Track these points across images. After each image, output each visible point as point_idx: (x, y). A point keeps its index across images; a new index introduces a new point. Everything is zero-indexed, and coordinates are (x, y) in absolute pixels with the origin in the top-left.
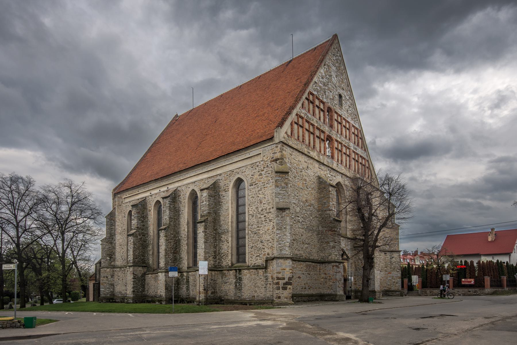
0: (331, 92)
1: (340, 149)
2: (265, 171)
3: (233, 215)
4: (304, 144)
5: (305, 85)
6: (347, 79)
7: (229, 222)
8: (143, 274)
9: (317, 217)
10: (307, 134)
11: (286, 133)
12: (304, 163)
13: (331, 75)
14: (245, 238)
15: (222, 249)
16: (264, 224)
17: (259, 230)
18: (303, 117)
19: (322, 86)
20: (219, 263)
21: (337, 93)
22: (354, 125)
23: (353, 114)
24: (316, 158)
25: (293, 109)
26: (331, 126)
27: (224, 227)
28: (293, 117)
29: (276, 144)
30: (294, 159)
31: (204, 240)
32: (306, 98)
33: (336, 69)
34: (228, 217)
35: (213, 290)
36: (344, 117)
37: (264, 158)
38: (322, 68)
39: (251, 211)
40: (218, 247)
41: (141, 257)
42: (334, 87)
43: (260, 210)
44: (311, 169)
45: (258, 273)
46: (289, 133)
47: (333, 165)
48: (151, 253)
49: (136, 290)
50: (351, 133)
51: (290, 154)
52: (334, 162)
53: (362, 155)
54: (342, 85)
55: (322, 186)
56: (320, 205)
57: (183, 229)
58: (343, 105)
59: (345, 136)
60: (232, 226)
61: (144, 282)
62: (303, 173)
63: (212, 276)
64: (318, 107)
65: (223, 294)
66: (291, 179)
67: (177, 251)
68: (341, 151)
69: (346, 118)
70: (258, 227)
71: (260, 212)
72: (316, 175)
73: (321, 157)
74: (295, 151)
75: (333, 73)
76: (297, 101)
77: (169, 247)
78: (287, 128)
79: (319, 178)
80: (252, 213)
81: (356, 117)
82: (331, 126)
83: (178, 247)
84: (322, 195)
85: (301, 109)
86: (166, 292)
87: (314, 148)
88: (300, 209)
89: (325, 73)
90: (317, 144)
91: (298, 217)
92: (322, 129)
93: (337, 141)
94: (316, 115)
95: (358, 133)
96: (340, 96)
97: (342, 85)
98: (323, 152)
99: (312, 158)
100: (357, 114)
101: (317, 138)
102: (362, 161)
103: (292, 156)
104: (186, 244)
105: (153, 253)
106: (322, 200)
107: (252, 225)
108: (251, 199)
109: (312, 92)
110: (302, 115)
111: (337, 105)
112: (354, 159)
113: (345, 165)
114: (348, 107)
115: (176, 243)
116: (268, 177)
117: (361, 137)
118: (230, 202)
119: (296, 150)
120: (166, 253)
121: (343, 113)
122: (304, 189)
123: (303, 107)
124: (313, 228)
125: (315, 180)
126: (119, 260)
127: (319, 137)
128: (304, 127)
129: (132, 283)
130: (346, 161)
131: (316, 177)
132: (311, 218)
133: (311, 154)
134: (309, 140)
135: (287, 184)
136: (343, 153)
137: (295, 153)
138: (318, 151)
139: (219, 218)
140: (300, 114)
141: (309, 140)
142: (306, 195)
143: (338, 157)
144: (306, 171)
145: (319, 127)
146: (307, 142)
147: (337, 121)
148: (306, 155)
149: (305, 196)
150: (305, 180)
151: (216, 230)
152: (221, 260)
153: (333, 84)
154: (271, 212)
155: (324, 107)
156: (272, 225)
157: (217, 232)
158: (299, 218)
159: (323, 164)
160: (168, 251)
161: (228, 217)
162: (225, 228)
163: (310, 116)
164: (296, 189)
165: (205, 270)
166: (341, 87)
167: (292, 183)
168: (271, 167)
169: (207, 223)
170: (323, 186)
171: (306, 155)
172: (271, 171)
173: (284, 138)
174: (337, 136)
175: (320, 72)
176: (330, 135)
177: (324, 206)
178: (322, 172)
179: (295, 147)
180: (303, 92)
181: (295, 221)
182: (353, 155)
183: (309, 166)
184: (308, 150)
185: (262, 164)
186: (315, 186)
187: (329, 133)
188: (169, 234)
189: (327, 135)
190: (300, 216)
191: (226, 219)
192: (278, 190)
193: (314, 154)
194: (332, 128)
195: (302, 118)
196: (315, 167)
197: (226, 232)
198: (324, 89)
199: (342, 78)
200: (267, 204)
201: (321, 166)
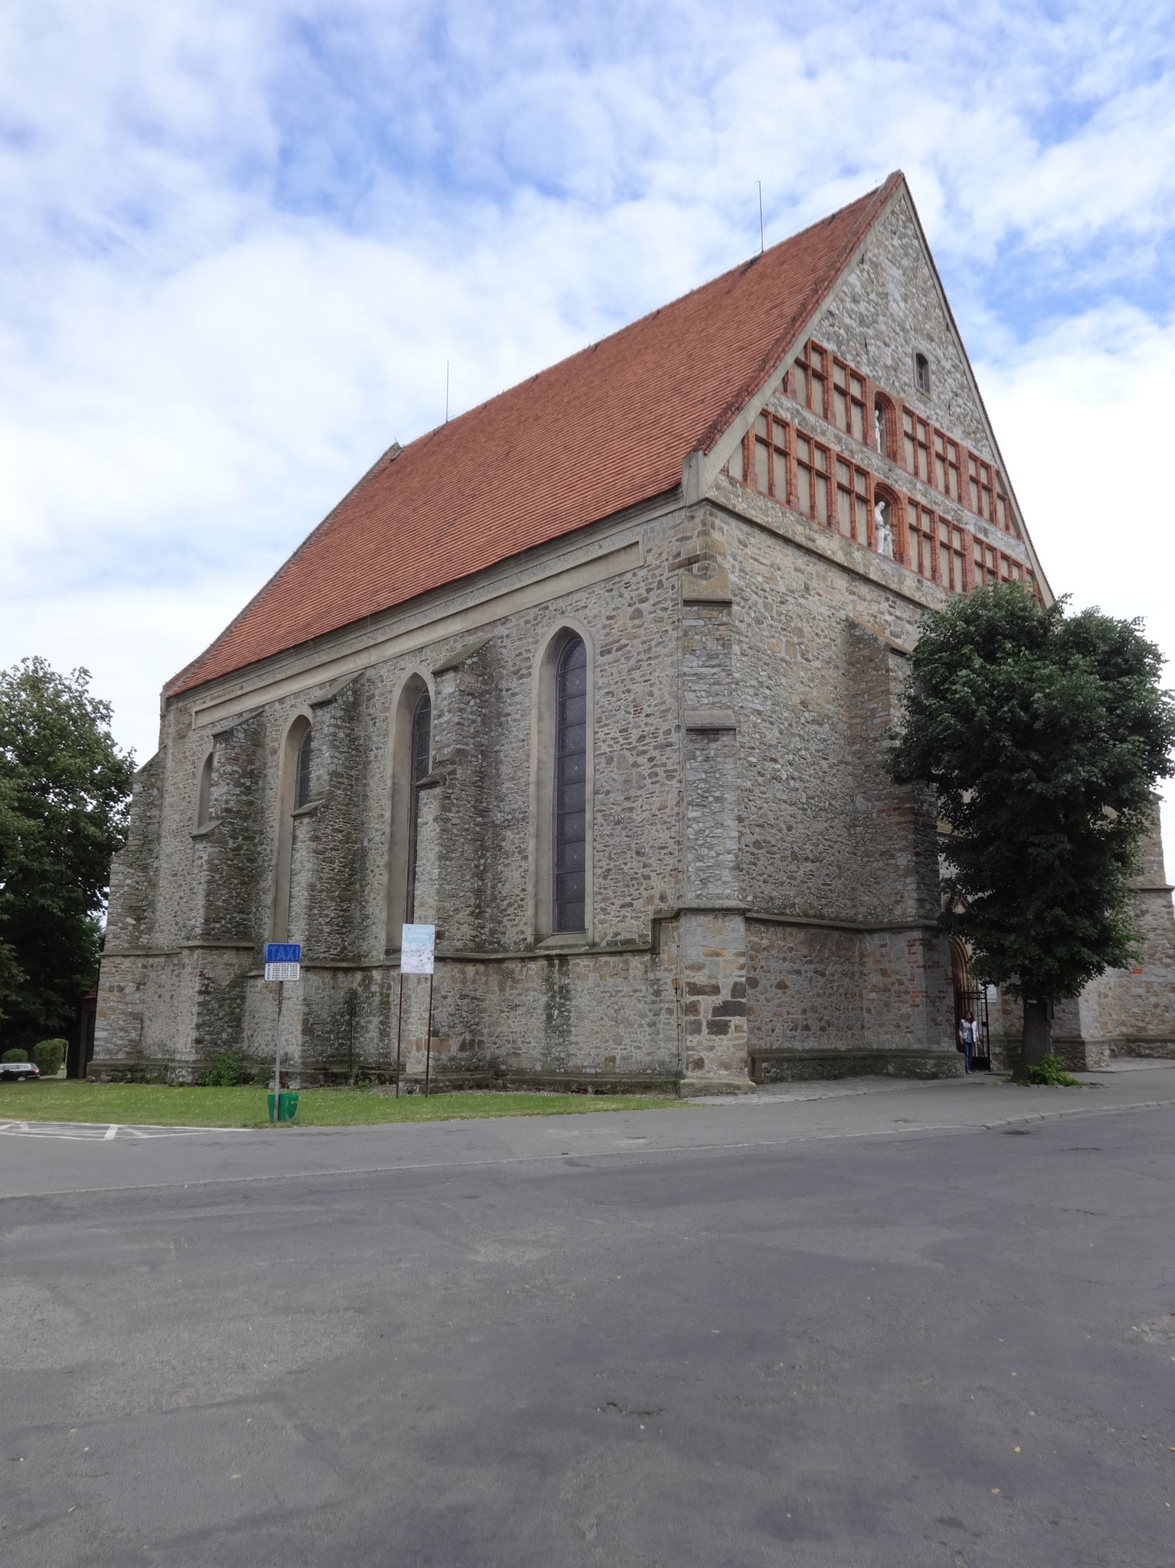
0: (886, 345)
1: (928, 531)
2: (651, 601)
3: (544, 757)
4: (791, 509)
5: (794, 320)
6: (942, 308)
7: (528, 784)
8: (237, 977)
9: (847, 764)
10: (802, 478)
11: (725, 471)
12: (794, 574)
13: (887, 294)
14: (584, 840)
15: (505, 881)
16: (649, 786)
17: (631, 809)
18: (788, 420)
19: (854, 325)
20: (493, 932)
21: (909, 350)
22: (976, 452)
23: (968, 418)
24: (840, 558)
25: (751, 394)
26: (892, 455)
27: (514, 802)
28: (748, 419)
29: (690, 507)
30: (757, 560)
31: (437, 848)
32: (798, 362)
33: (904, 275)
34: (526, 764)
35: (468, 1037)
36: (938, 426)
37: (651, 559)
38: (853, 271)
39: (604, 741)
40: (489, 875)
41: (235, 915)
42: (898, 329)
43: (634, 739)
44: (819, 595)
45: (627, 970)
46: (737, 472)
47: (901, 582)
48: (268, 899)
49: (207, 1037)
50: (965, 478)
51: (740, 542)
52: (907, 573)
53: (1008, 552)
54: (927, 326)
55: (861, 653)
56: (858, 721)
57: (374, 814)
58: (932, 387)
59: (942, 488)
60: (538, 799)
61: (239, 1006)
62: (791, 607)
63: (464, 982)
64: (843, 393)
65: (503, 1052)
66: (743, 626)
67: (355, 893)
68: (930, 537)
69: (944, 431)
70: (628, 799)
71: (634, 744)
72: (837, 614)
73: (857, 555)
74: (757, 533)
75: (891, 288)
76: (765, 365)
77: (325, 876)
78: (726, 456)
79: (851, 625)
80: (608, 750)
81: (980, 427)
82: (892, 455)
83: (358, 877)
84: (863, 686)
85: (777, 394)
86: (304, 1044)
87: (829, 524)
88: (781, 733)
89: (864, 287)
90: (839, 509)
91: (774, 760)
92: (859, 463)
93: (914, 503)
94: (834, 415)
95: (989, 479)
96: (921, 360)
97: (927, 326)
98: (862, 539)
99: (822, 557)
100: (984, 419)
101: (840, 493)
102: (1010, 572)
103: (747, 550)
104: (385, 866)
105: (276, 900)
106: (863, 703)
107: (608, 793)
108: (604, 701)
109: (820, 343)
110: (785, 415)
111: (909, 386)
112: (981, 566)
113: (946, 583)
114: (951, 395)
115: (353, 862)
116: (661, 620)
117: (1001, 493)
118: (534, 712)
119: (763, 528)
120: (312, 898)
121: (936, 417)
122: (796, 663)
123: (785, 390)
124: (833, 802)
125: (837, 633)
126: (166, 928)
127: (846, 490)
128: (793, 453)
129: (195, 1009)
130: (951, 570)
131: (838, 623)
132: (824, 764)
133: (818, 542)
134: (812, 497)
135: (726, 644)
136: (938, 544)
137: (759, 538)
138: (843, 536)
139: (497, 770)
140: (777, 411)
141: (812, 497)
142: (802, 683)
143: (920, 556)
144: (801, 600)
145: (846, 455)
146: (804, 504)
147: (913, 439)
148: (799, 546)
149: (798, 685)
150: (800, 632)
151: (483, 812)
152: (500, 922)
153: (894, 320)
154: (670, 745)
155: (863, 393)
156: (676, 791)
157: (486, 820)
158: (779, 766)
159: (866, 580)
160: (321, 891)
161: (526, 764)
162: (516, 807)
163: (811, 418)
164: (766, 664)
165: (425, 957)
166: (922, 330)
167: (747, 640)
168: (673, 587)
169: (453, 786)
170: (866, 652)
171: (799, 546)
172: (673, 600)
173: (718, 487)
174: (915, 488)
175: (846, 282)
176: (889, 482)
177: (869, 723)
178: (862, 607)
179: (759, 521)
180: (784, 342)
181: (763, 776)
182: (976, 553)
183: (814, 584)
184: (808, 532)
185: (640, 580)
186: (836, 651)
187: (884, 475)
188: (328, 831)
189: (878, 484)
190: (782, 757)
191: (520, 774)
192: (695, 664)
193: (827, 544)
194: (895, 460)
195: (784, 425)
196: (833, 588)
197: (517, 820)
198: (861, 334)
199: (924, 302)
200: (657, 714)
201: (855, 586)
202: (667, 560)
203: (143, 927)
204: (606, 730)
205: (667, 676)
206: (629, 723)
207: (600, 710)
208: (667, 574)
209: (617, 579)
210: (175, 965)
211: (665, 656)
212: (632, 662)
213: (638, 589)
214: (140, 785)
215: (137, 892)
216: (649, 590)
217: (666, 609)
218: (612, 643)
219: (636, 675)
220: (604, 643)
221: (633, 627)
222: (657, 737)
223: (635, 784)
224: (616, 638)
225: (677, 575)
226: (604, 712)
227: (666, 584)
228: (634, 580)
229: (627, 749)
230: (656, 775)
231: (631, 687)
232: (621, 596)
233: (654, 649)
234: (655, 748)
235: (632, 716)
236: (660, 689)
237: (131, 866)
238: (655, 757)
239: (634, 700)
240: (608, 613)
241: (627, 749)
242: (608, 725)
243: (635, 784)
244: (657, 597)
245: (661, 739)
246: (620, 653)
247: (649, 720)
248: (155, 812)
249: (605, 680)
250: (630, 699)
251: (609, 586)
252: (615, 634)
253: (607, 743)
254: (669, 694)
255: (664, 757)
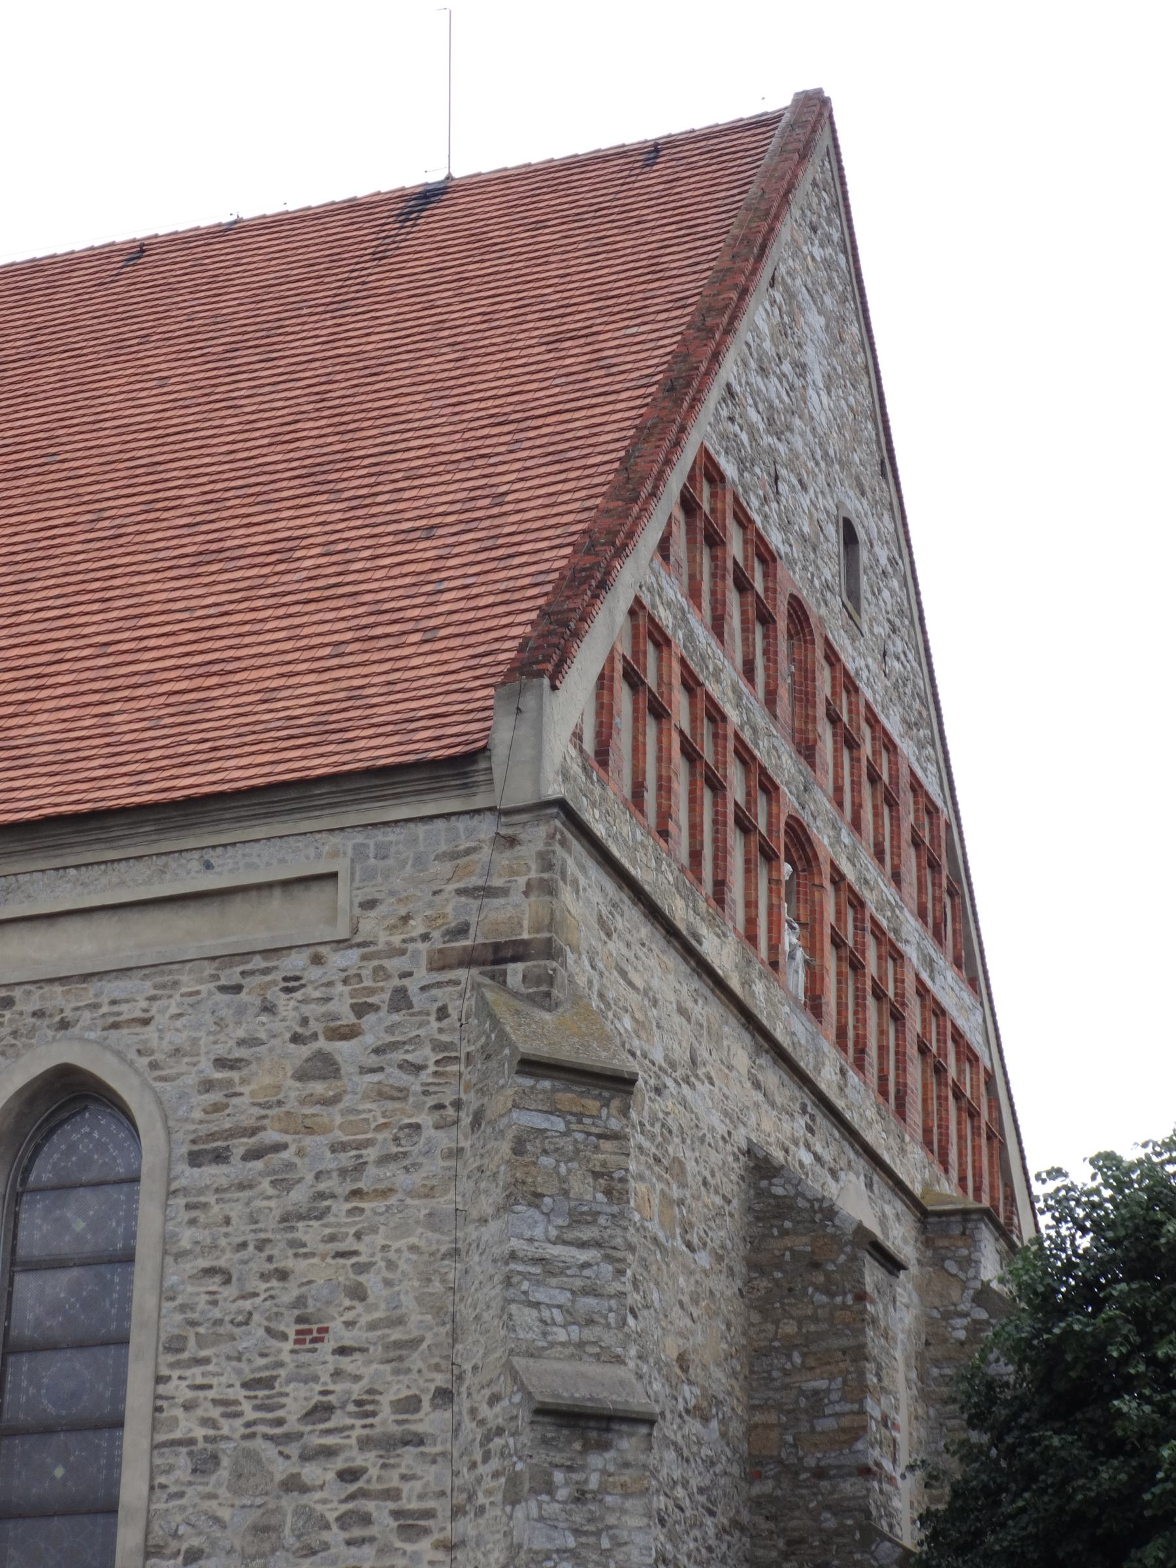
29: (508, 813)
37: (369, 925)
39: (188, 1407)
71: (293, 1424)
80: (199, 1433)
154: (418, 1440)
168: (442, 1013)
200: (376, 1351)
202: (425, 937)
204: (196, 1374)
205: (413, 1248)
206: (281, 1364)
207: (178, 1317)
208: (422, 976)
209: (258, 963)
211: (410, 1193)
212: (299, 1196)
213: (328, 999)
216: (361, 1010)
217: (418, 1068)
218: (232, 1134)
219: (310, 1233)
220: (204, 1130)
221: (303, 1102)
222: (374, 1414)
223: (290, 1540)
224: (248, 1122)
225: (456, 983)
226: (193, 1324)
227: (418, 1000)
228: (314, 973)
229: (266, 1437)
230: (366, 1519)
231: (290, 1263)
232: (269, 1009)
233: (371, 1170)
234: (365, 1444)
235: (289, 1345)
236: (388, 1283)
238: (364, 1471)
239: (300, 1301)
240: (221, 1051)
241: (266, 1437)
242: (206, 1361)
243: (290, 1540)
244: (390, 1029)
245: (386, 1420)
246: (259, 1165)
247: (345, 1363)
249: (203, 1235)
250: (287, 1298)
251: (231, 976)
252: (244, 1111)
253: (200, 1412)
254: (419, 1300)
255: (395, 1475)
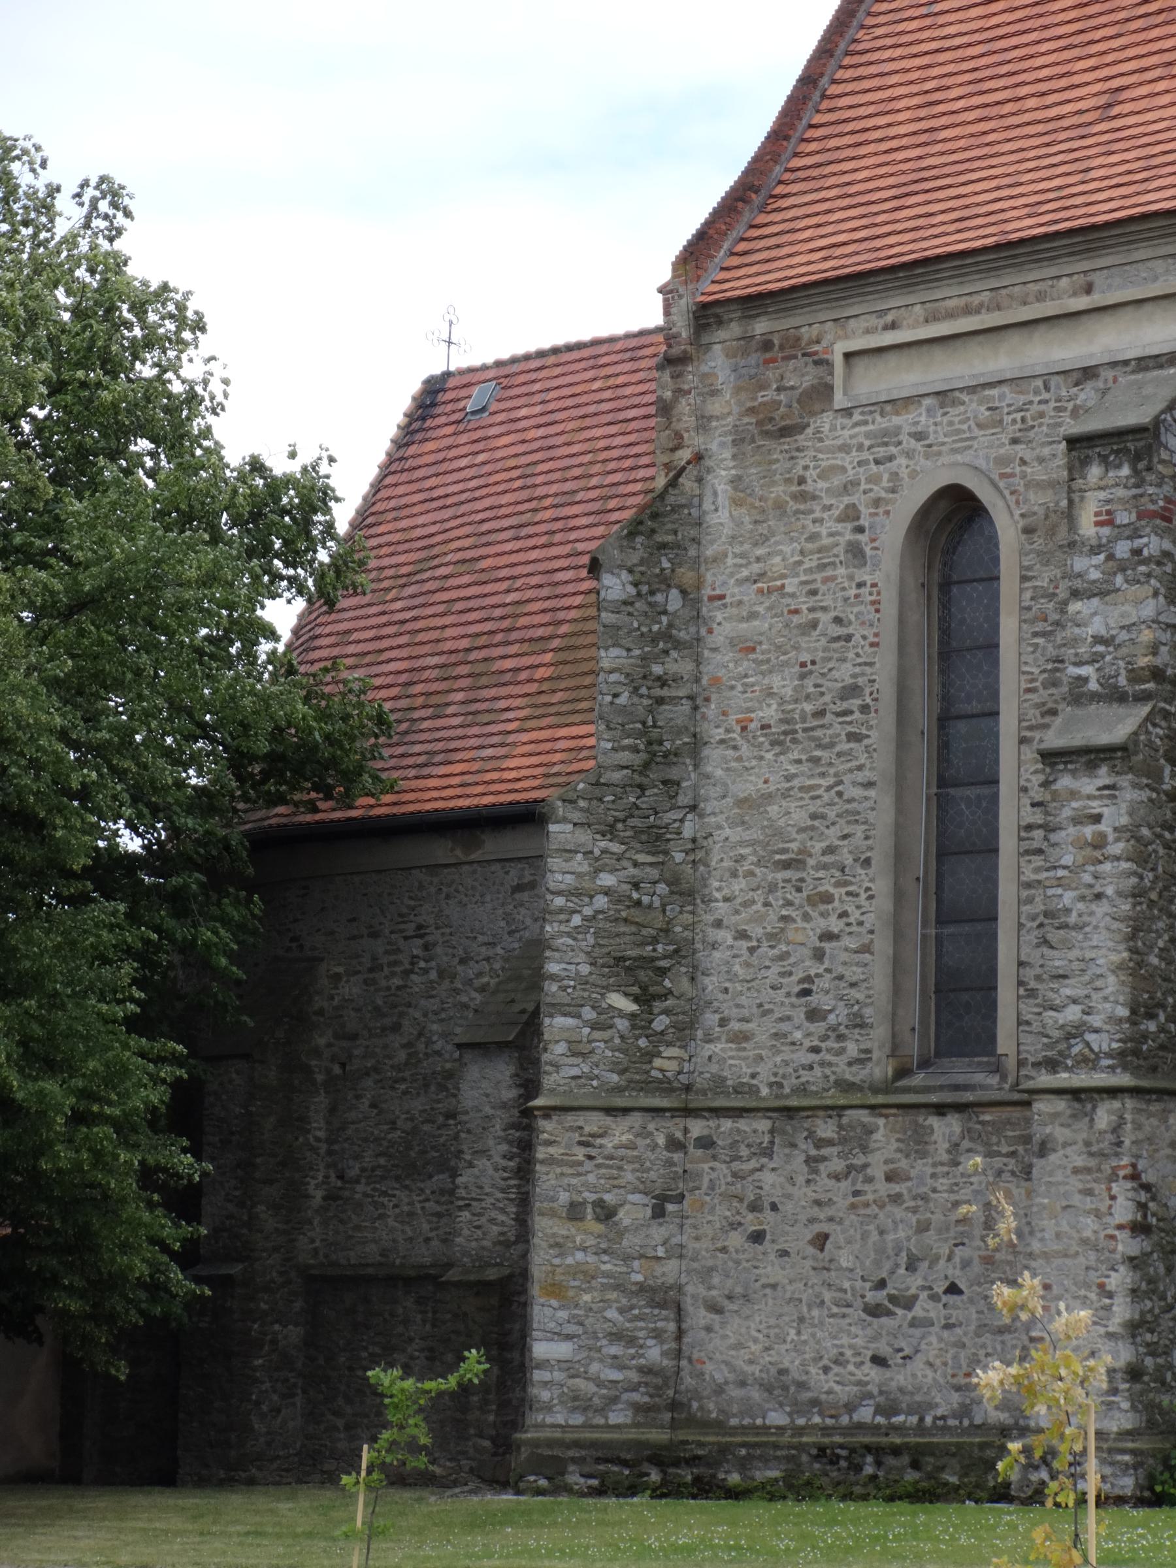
203: (661, 1022)
210: (820, 1143)
214: (625, 575)
215: (636, 915)
237: (610, 831)
248: (677, 665)
